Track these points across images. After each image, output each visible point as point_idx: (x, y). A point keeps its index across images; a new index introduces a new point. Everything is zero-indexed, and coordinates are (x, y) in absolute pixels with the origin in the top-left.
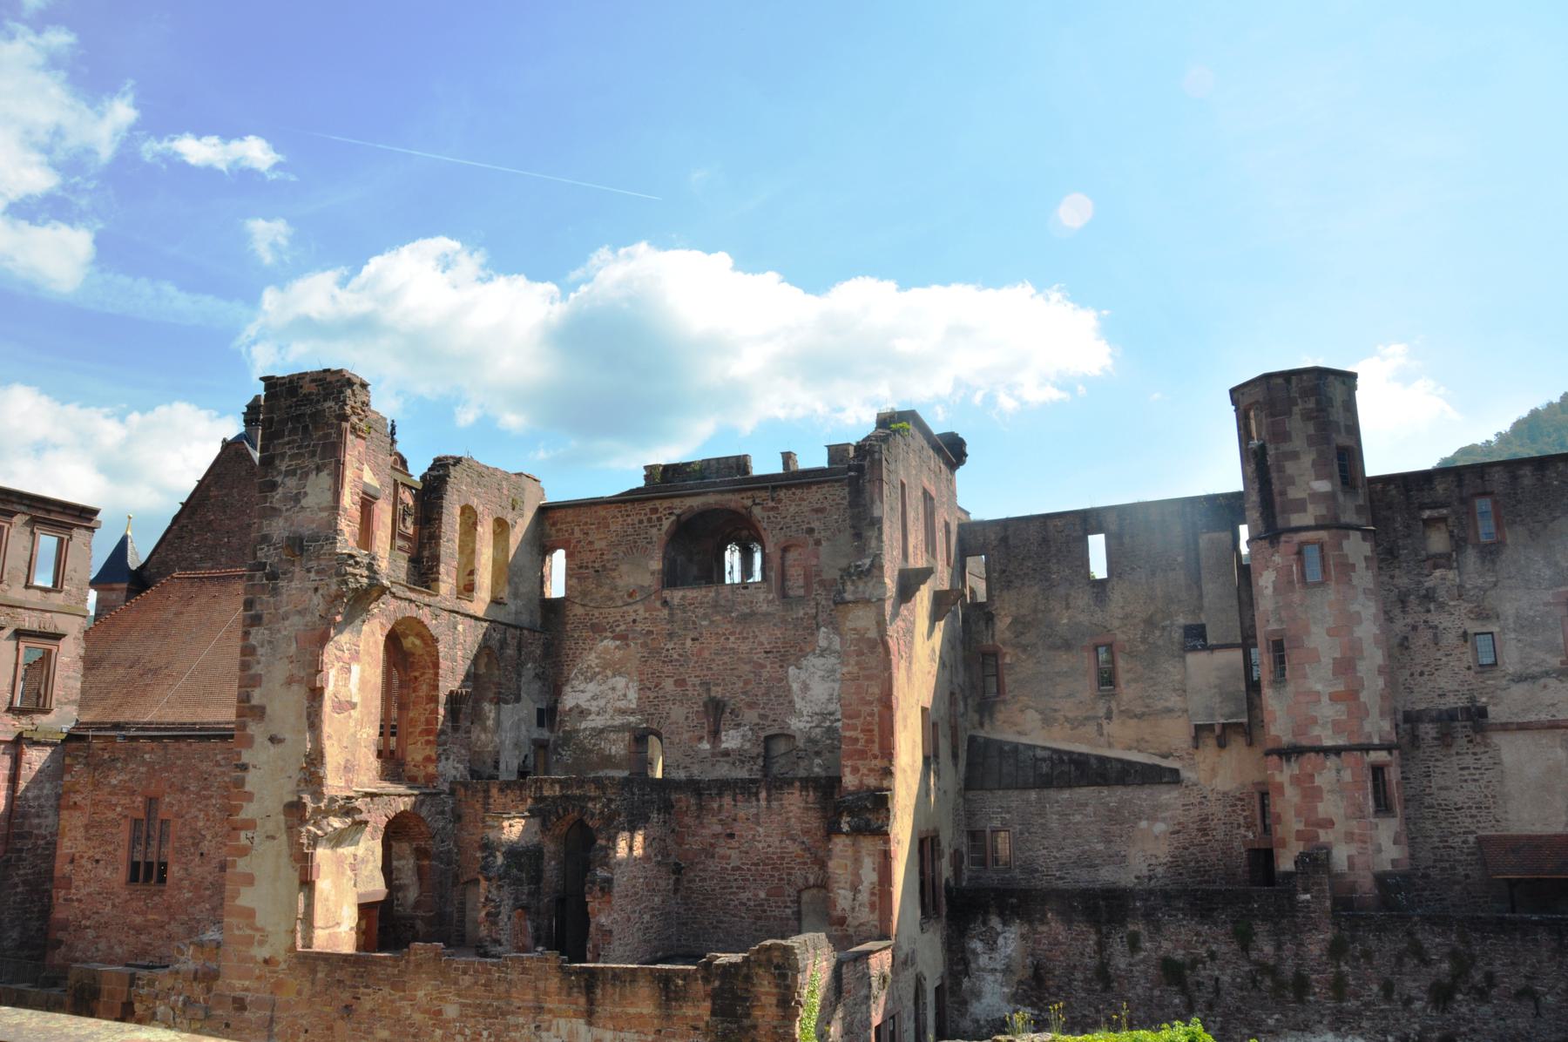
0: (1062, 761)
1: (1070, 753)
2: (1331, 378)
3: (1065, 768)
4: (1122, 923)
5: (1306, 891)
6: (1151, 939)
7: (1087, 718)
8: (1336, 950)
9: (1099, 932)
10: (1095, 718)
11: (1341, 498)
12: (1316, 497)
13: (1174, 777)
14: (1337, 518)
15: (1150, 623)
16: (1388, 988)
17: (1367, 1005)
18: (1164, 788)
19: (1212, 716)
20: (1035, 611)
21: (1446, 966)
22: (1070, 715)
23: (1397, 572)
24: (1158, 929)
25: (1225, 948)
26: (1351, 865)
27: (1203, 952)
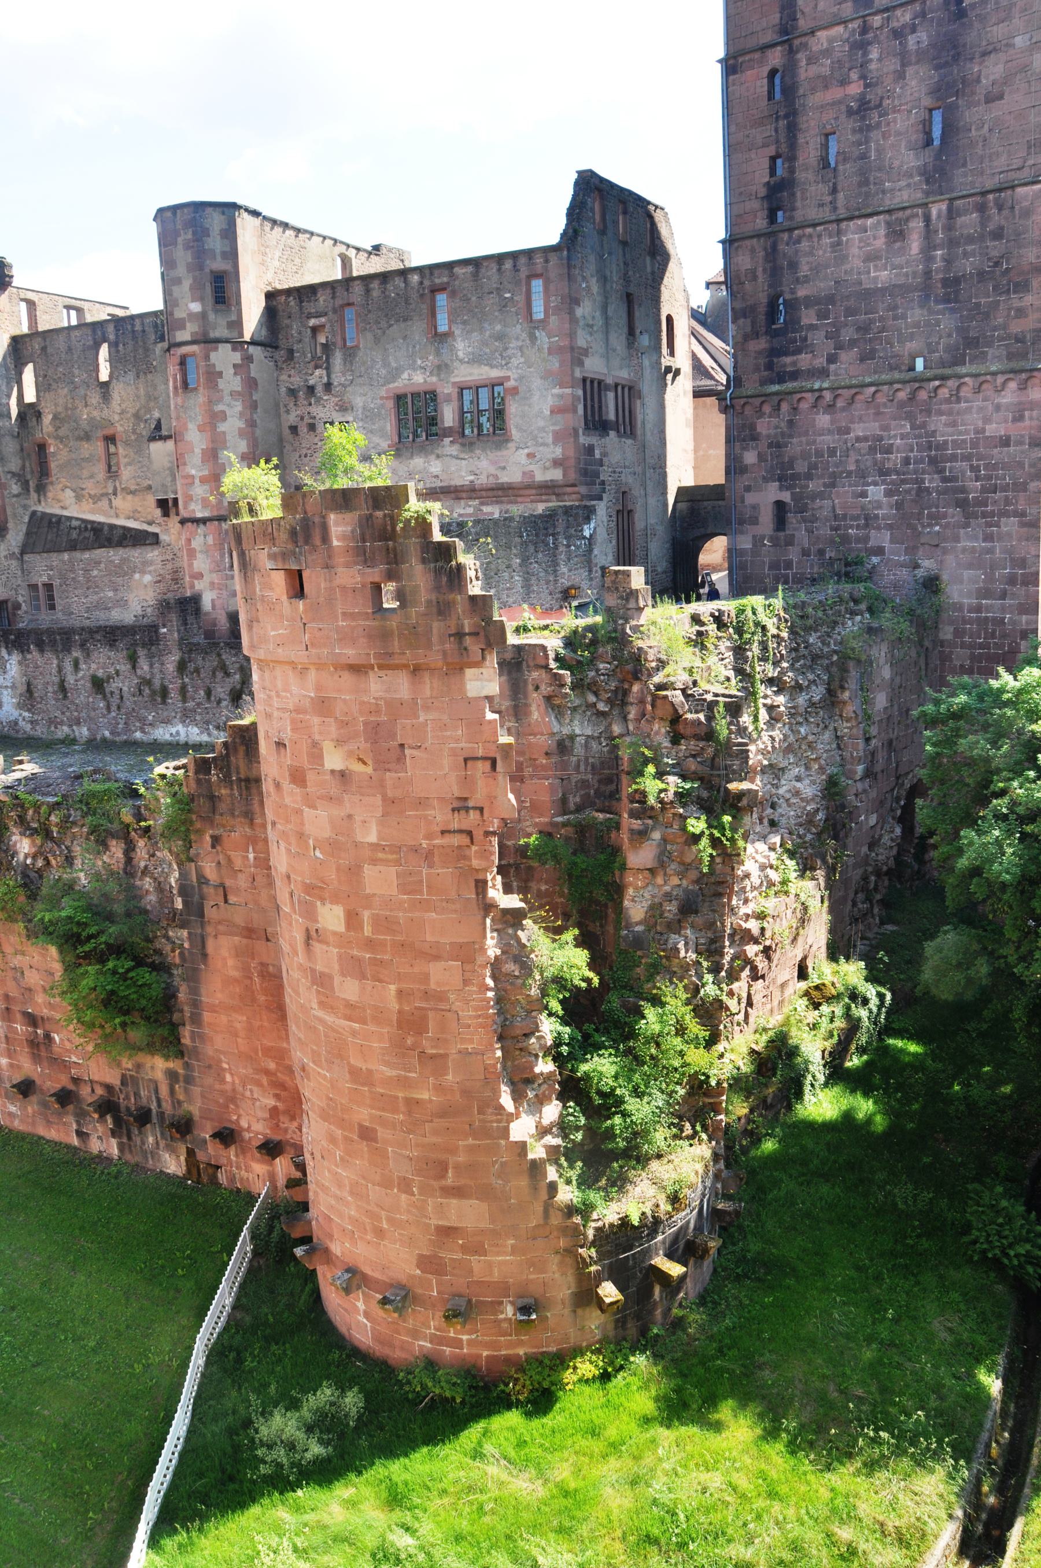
0: (86, 529)
1: (93, 522)
2: (209, 210)
3: (87, 534)
4: (69, 651)
5: (164, 626)
6: (85, 663)
7: (102, 495)
8: (182, 667)
9: (58, 658)
10: (107, 494)
11: (212, 316)
12: (192, 315)
13: (154, 540)
14: (205, 334)
15: (137, 416)
16: (209, 693)
17: (199, 704)
18: (149, 548)
19: (166, 493)
20: (66, 409)
21: (237, 677)
22: (92, 493)
23: (292, 372)
24: (88, 655)
25: (124, 667)
26: (214, 607)
27: (112, 670)
